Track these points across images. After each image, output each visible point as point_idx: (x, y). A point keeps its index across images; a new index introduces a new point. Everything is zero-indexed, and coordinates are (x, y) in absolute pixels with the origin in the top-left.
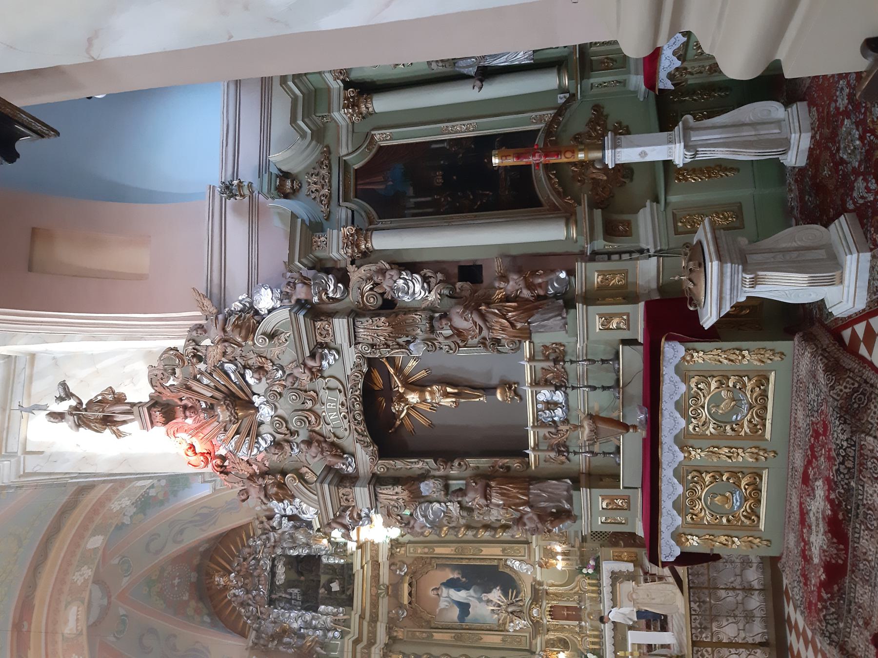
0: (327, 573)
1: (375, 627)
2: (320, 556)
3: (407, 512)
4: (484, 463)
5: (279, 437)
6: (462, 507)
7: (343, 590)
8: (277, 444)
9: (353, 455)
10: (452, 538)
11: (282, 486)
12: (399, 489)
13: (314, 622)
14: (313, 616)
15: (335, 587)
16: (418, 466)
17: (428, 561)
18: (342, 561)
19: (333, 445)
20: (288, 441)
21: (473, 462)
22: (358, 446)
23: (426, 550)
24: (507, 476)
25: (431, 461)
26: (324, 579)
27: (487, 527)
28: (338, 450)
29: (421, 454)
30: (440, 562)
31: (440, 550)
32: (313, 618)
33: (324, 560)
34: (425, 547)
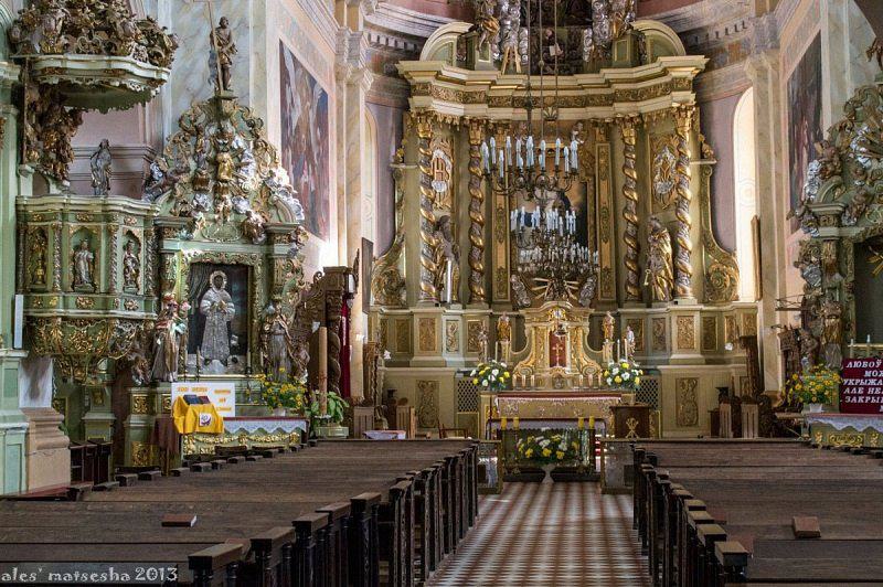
0: (570, 37)
1: (508, 106)
2: (589, 25)
3: (813, 259)
4: (852, 314)
5: (870, 172)
6: (818, 297)
7: (549, 61)
8: (865, 171)
9: (856, 224)
10: (622, 203)
11: (833, 174)
12: (833, 257)
13: (509, 23)
14: (516, 22)
15: (554, 50)
16: (850, 269)
17: (590, 172)
18: (586, 58)
19: (865, 211)
20: (866, 179)
21: (852, 307)
22: (863, 229)
23: (603, 169)
24: (844, 327)
25: (852, 279)
26: (564, 32)
27: (638, 249)
28: (860, 215)
29: (857, 273)
30: (590, 188)
31: (604, 186)
32: (513, 23)
33: (587, 33)
34: (607, 168)
